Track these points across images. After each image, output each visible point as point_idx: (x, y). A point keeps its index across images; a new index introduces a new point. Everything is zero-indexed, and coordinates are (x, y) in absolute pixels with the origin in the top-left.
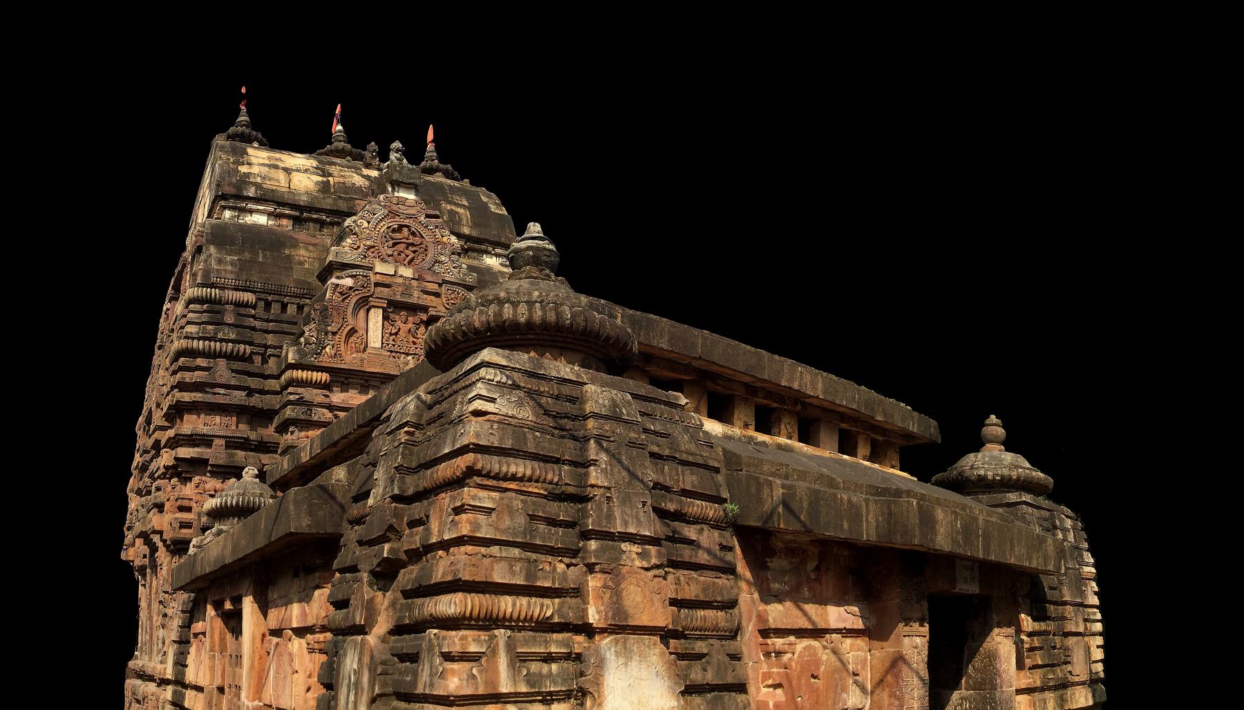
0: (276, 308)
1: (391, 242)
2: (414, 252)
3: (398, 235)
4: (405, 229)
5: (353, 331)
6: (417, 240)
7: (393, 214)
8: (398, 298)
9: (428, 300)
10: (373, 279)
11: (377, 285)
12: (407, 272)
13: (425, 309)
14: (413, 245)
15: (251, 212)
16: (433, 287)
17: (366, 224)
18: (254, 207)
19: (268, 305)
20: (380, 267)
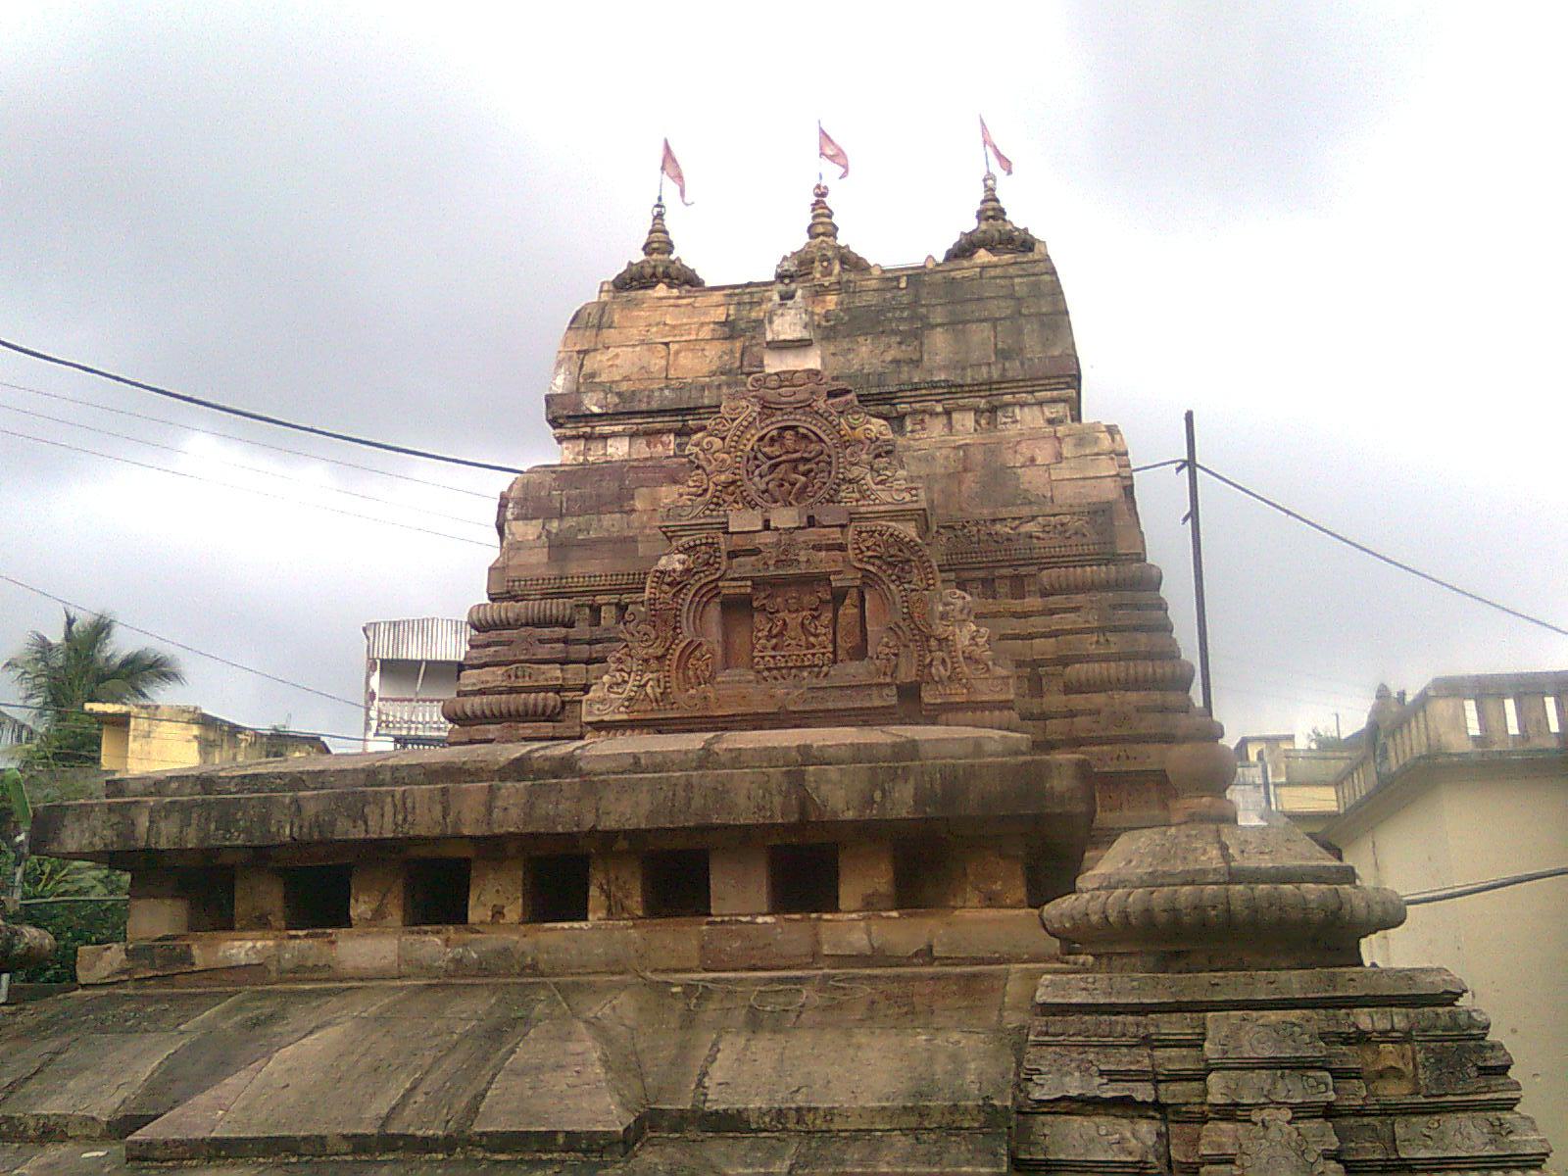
0: (608, 615)
1: (765, 467)
2: (805, 474)
3: (775, 450)
4: (789, 434)
5: (693, 648)
6: (815, 447)
7: (767, 408)
8: (772, 571)
9: (824, 561)
10: (724, 544)
11: (732, 555)
12: (785, 517)
13: (824, 579)
14: (807, 460)
15: (604, 437)
16: (835, 535)
17: (718, 443)
18: (607, 429)
19: (596, 610)
20: (743, 520)
